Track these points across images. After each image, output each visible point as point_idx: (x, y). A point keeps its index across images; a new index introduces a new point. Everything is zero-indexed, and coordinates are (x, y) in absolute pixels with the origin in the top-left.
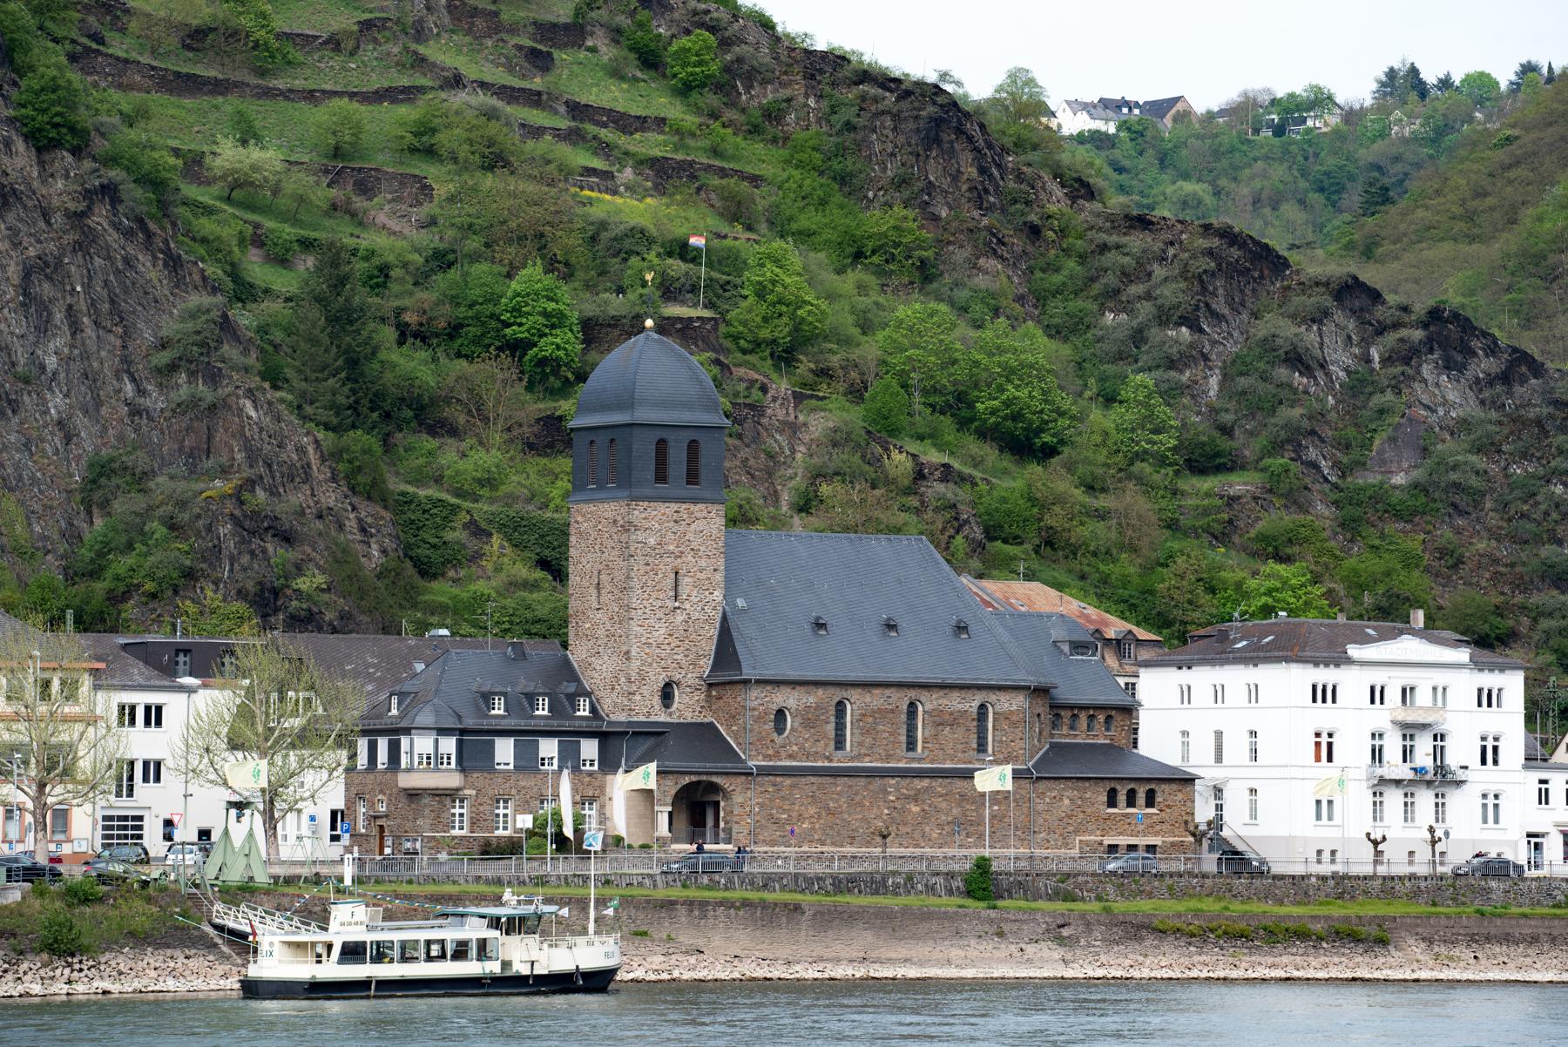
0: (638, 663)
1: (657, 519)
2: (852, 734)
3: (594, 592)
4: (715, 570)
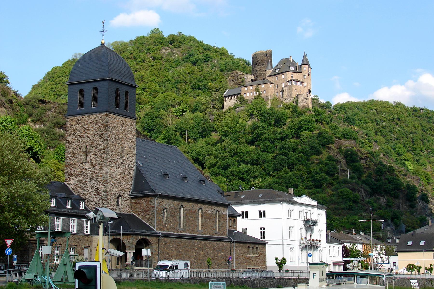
2: (183, 221)
3: (83, 155)
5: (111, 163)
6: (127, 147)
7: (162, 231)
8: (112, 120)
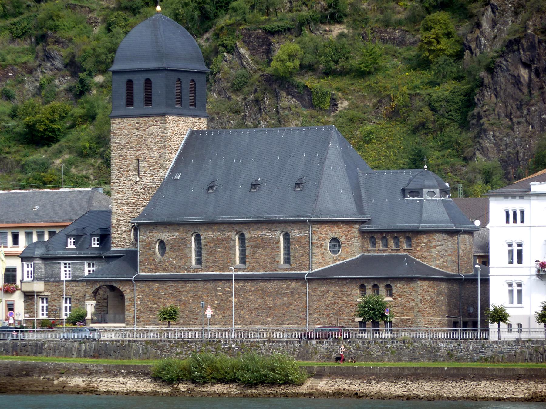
0: (117, 215)
1: (126, 128)
4: (160, 157)
5: (117, 185)
6: (149, 157)
7: (153, 272)
8: (118, 127)
